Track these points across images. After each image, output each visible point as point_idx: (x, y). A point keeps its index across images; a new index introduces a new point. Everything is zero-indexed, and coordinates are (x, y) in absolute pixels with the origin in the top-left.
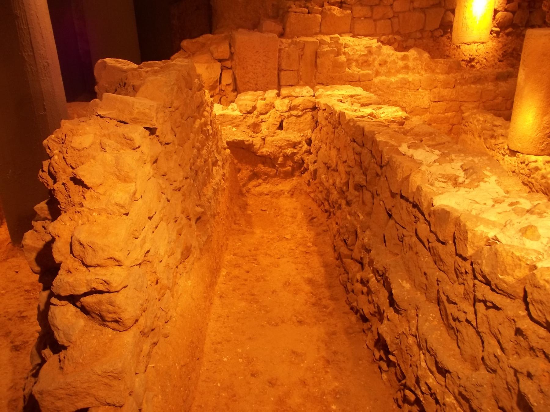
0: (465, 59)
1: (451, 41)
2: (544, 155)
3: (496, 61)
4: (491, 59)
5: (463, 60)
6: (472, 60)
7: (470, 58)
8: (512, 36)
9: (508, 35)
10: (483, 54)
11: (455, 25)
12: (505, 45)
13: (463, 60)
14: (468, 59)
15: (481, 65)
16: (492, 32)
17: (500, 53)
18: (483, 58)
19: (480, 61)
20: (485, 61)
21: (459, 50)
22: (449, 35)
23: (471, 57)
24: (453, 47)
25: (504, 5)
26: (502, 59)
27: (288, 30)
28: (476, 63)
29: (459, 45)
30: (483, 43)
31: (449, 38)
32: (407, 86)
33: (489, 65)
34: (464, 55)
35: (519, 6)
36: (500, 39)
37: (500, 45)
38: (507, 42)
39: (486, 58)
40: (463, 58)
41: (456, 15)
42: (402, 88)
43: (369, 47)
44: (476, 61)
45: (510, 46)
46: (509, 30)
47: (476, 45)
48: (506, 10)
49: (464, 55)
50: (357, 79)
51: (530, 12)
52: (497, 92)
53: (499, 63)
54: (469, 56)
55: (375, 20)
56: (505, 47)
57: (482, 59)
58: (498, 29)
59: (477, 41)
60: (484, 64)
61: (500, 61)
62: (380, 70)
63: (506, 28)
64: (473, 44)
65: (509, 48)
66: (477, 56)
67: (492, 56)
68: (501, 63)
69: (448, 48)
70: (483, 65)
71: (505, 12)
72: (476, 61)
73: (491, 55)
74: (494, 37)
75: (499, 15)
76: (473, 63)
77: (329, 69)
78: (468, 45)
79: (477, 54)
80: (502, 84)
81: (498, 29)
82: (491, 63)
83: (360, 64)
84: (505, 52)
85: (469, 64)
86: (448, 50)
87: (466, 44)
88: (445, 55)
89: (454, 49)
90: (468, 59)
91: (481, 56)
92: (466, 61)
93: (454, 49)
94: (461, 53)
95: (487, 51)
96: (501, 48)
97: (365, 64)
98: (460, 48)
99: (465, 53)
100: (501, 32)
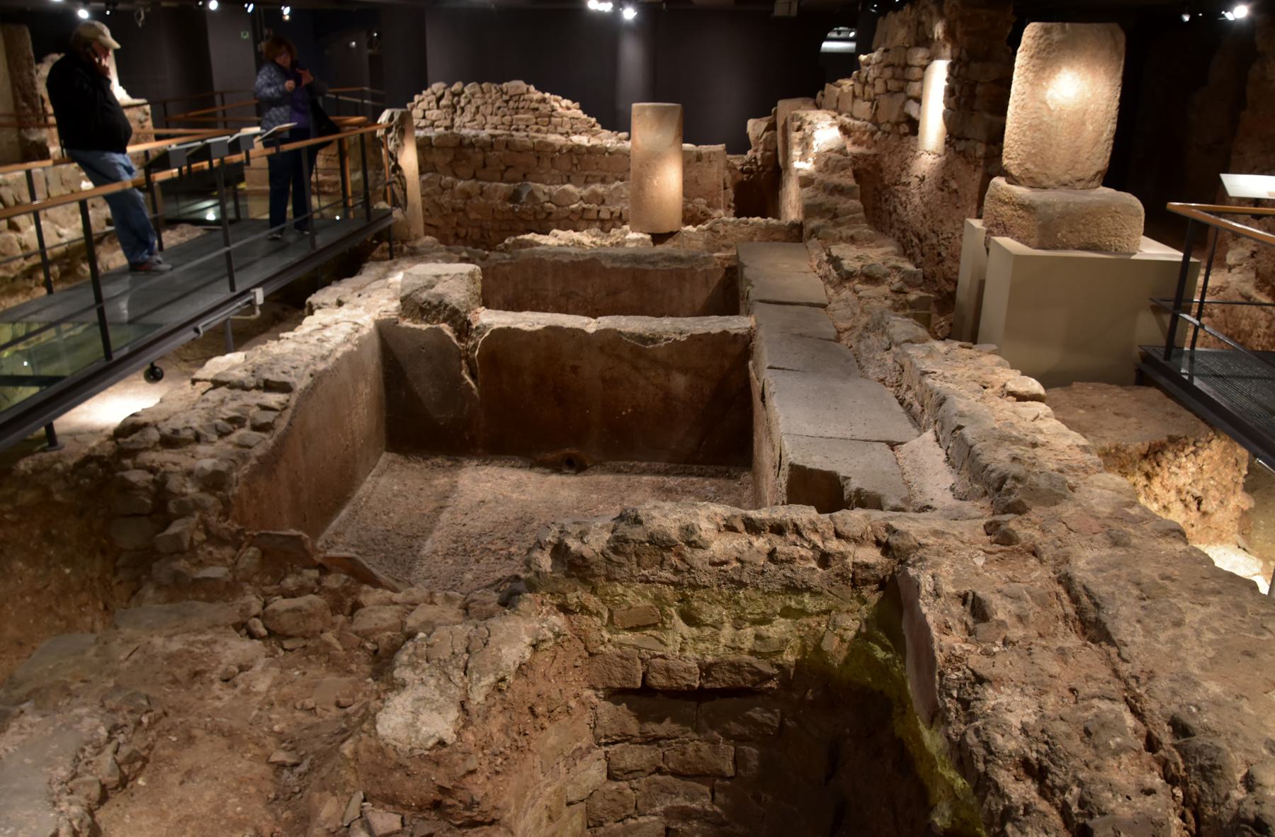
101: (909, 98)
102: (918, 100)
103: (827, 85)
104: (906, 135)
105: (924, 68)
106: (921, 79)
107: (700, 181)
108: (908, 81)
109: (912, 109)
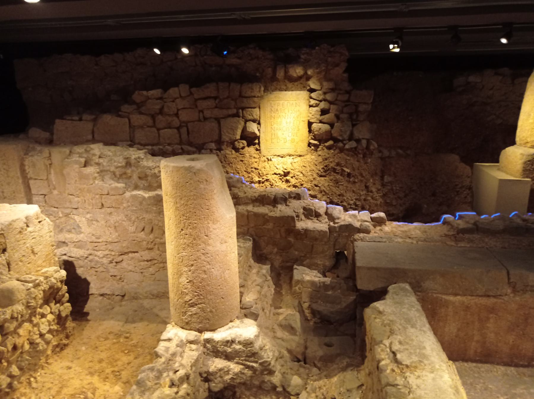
1: (260, 153)
2: (190, 330)
3: (315, 176)
4: (309, 173)
5: (275, 174)
6: (286, 174)
7: (284, 172)
8: (334, 150)
9: (329, 148)
10: (300, 168)
12: (326, 159)
13: (275, 174)
14: (282, 173)
16: (309, 145)
17: (320, 167)
19: (295, 175)
20: (302, 175)
21: (270, 162)
23: (285, 171)
25: (318, 117)
26: (324, 174)
27: (55, 137)
30: (300, 156)
33: (306, 180)
34: (277, 168)
35: (337, 117)
36: (320, 153)
37: (320, 159)
38: (328, 156)
40: (275, 172)
43: (127, 158)
44: (291, 175)
45: (331, 160)
46: (330, 143)
47: (292, 157)
48: (321, 122)
49: (277, 168)
50: (106, 193)
51: (353, 125)
53: (319, 178)
54: (282, 169)
55: (158, 130)
56: (326, 161)
57: (299, 174)
58: (316, 142)
59: (293, 154)
61: (321, 176)
62: (139, 184)
63: (326, 141)
64: (288, 157)
65: (331, 162)
67: (310, 171)
68: (322, 178)
69: (256, 160)
70: (299, 180)
71: (320, 124)
73: (308, 169)
74: (312, 150)
76: (288, 178)
77: (76, 180)
78: (282, 157)
79: (292, 168)
81: (316, 142)
82: (308, 178)
83: (118, 176)
84: (326, 166)
85: (285, 178)
87: (279, 156)
89: (265, 161)
90: (282, 173)
91: (297, 170)
92: (279, 174)
95: (304, 165)
96: (321, 162)
97: (124, 176)
98: (271, 160)
99: (278, 167)
100: (320, 145)
101: (246, 121)
103: (57, 121)
107: (36, 250)
108: (243, 109)
109: (253, 127)
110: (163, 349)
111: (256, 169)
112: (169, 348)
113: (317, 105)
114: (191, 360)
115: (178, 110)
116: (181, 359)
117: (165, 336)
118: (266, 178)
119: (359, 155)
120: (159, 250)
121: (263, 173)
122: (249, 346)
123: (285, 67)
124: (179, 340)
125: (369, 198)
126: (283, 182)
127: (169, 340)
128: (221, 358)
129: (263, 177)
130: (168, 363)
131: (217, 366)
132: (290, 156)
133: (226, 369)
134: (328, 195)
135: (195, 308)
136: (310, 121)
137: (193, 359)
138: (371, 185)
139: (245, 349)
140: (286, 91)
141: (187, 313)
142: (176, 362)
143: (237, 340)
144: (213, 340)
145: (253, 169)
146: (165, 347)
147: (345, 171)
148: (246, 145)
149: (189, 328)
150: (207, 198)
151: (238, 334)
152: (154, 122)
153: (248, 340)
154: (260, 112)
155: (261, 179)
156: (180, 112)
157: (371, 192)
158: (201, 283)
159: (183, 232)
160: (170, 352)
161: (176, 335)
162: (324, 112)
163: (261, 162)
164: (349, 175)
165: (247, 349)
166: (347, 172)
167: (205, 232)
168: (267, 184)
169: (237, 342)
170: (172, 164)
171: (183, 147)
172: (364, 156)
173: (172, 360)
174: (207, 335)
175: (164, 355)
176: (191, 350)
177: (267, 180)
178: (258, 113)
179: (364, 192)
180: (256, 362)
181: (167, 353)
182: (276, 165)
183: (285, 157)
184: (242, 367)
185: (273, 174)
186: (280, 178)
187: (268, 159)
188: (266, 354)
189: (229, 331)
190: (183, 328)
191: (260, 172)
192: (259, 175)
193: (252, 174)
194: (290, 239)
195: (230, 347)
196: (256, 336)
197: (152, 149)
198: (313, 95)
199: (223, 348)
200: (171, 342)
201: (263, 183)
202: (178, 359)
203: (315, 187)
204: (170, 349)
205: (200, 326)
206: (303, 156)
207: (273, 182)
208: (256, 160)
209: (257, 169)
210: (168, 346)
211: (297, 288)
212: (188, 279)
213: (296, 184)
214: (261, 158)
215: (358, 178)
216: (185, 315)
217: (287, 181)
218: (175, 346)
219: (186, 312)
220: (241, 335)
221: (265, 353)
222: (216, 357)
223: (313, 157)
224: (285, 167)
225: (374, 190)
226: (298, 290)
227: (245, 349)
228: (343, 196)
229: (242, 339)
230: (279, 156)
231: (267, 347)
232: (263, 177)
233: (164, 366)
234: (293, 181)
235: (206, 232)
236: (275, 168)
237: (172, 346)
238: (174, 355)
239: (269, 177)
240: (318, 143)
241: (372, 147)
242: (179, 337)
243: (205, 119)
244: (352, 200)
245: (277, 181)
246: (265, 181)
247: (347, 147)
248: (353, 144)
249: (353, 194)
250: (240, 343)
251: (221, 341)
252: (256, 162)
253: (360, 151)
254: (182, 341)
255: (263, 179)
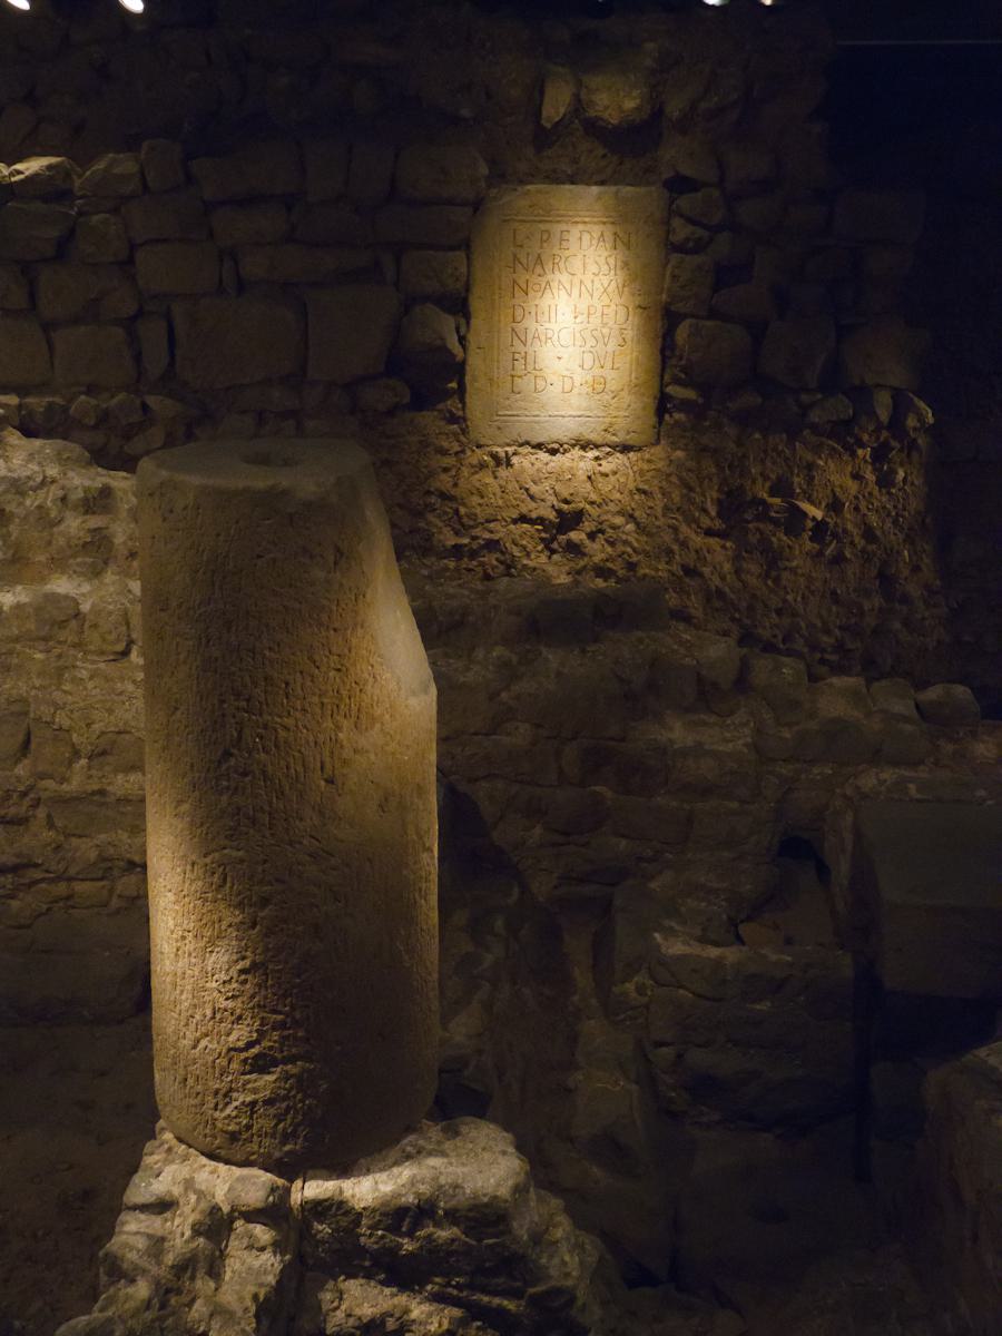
0: (534, 515)
1: (464, 432)
5: (523, 519)
6: (570, 519)
7: (559, 512)
10: (625, 499)
11: (475, 362)
13: (523, 519)
14: (552, 515)
15: (612, 544)
16: (663, 405)
18: (620, 513)
19: (604, 526)
20: (630, 527)
21: (503, 472)
22: (452, 404)
23: (565, 507)
24: (474, 457)
28: (592, 536)
29: (500, 451)
30: (625, 449)
31: (453, 419)
32: (68, 635)
39: (637, 514)
40: (524, 510)
41: (477, 322)
42: (45, 639)
44: (588, 526)
47: (595, 453)
48: (713, 314)
49: (532, 497)
52: (504, 695)
54: (552, 500)
55: (48, 327)
57: (619, 520)
58: (690, 394)
59: (594, 437)
60: (626, 543)
64: (577, 452)
66: (592, 503)
69: (448, 461)
70: (620, 548)
72: (588, 526)
75: (682, 333)
76: (574, 536)
78: (553, 452)
79: (593, 497)
80: (552, 658)
81: (690, 394)
85: (562, 538)
86: (446, 470)
87: (539, 446)
88: (429, 493)
89: (482, 466)
90: (552, 515)
91: (612, 507)
92: (541, 520)
93: (482, 466)
94: (512, 486)
98: (509, 464)
99: (534, 489)
102: (459, 306)
104: (391, 413)
105: (477, 206)
106: (466, 246)
110: (141, 1243)
111: (444, 496)
112: (163, 1239)
113: (698, 247)
114: (252, 1289)
115: (133, 247)
116: (212, 1285)
117: (145, 1188)
118: (487, 535)
119: (860, 452)
120: (51, 825)
121: (473, 517)
122: (490, 1230)
123: (579, 84)
124: (203, 1205)
125: (897, 625)
126: (553, 552)
127: (163, 1206)
128: (369, 1276)
129: (477, 532)
130: (163, 1306)
131: (358, 1312)
132: (584, 448)
133: (391, 1324)
134: (738, 610)
135: (271, 1078)
136: (673, 308)
137: (261, 1285)
138: (906, 572)
139: (474, 1243)
140: (573, 183)
141: (235, 1095)
142: (193, 1301)
143: (442, 1204)
144: (341, 1203)
145: (433, 499)
146: (149, 1236)
147: (805, 514)
148: (407, 400)
149: (239, 1157)
150: (336, 625)
151: (442, 1180)
152: (32, 297)
153: (486, 1205)
154: (469, 266)
155: (466, 541)
156: (140, 256)
157: (905, 599)
158: (299, 976)
159: (232, 762)
160: (169, 1259)
161: (189, 1184)
162: (724, 276)
163: (465, 472)
164: (820, 529)
165: (479, 1240)
166: (814, 519)
167: (322, 764)
168: (491, 559)
169: (441, 1212)
170: (196, 480)
171: (151, 400)
172: (879, 456)
173: (179, 1292)
174: (314, 1189)
175: (144, 1271)
176: (250, 1247)
177: (492, 545)
178: (464, 270)
179: (877, 601)
180: (514, 1294)
181: (159, 1263)
182: (530, 485)
183: (565, 451)
184: (457, 1312)
185: (515, 522)
186: (543, 535)
187: (494, 456)
188: (556, 1261)
189: (405, 1172)
190: (212, 1156)
191: (462, 510)
192: (460, 525)
193: (431, 517)
194: (597, 788)
195: (410, 1234)
196: (517, 1189)
197: (20, 406)
198: (684, 202)
199: (383, 1237)
200: (168, 1215)
201: (473, 554)
202: (204, 1285)
203: (687, 580)
204: (166, 1245)
205: (287, 1148)
206: (640, 449)
207: (516, 552)
208: (448, 461)
209: (452, 498)
210: (160, 1233)
211: (630, 987)
212: (244, 958)
213: (609, 565)
214: (469, 453)
215: (852, 543)
216: (227, 1104)
217: (574, 549)
218: (188, 1233)
219: (231, 1090)
220: (456, 1186)
221: (551, 1257)
222: (350, 1276)
223: (679, 454)
224: (565, 494)
225: (914, 590)
226: (634, 995)
227: (474, 1243)
228: (794, 614)
229: (461, 1201)
230: (539, 446)
231: (559, 1233)
232: (477, 532)
233: (149, 1315)
234: (598, 551)
235: (328, 766)
236: (525, 496)
237: (180, 1229)
238: (185, 1267)
239: (500, 531)
240: (700, 401)
241: (911, 422)
242: (201, 1194)
243: (241, 287)
244: (828, 632)
245: (530, 547)
246: (482, 547)
247: (815, 416)
248: (841, 407)
249: (834, 609)
250: (452, 1217)
251: (374, 1210)
252: (446, 470)
253: (866, 437)
254: (215, 1210)
255: (474, 538)
